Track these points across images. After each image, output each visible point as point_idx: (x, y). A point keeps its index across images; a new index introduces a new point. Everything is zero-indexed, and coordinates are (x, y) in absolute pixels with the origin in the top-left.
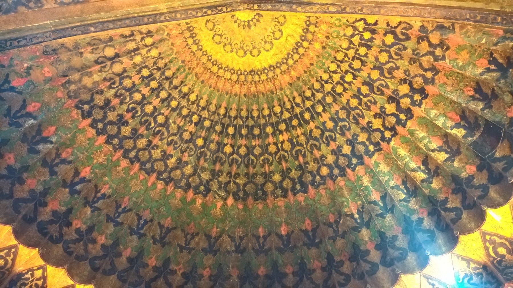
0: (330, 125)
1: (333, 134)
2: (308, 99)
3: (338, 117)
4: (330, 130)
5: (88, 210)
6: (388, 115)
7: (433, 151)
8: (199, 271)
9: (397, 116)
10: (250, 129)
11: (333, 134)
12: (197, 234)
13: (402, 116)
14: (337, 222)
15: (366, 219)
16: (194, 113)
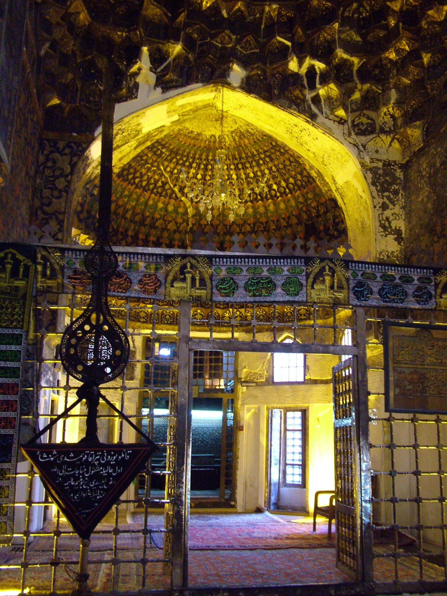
0: (252, 175)
1: (252, 181)
2: (243, 158)
3: (257, 174)
4: (251, 178)
5: (123, 221)
6: (281, 187)
7: (293, 215)
8: (173, 243)
9: (285, 189)
10: (206, 166)
11: (252, 181)
12: (171, 221)
13: (287, 190)
14: (242, 225)
15: (256, 230)
16: (173, 158)
